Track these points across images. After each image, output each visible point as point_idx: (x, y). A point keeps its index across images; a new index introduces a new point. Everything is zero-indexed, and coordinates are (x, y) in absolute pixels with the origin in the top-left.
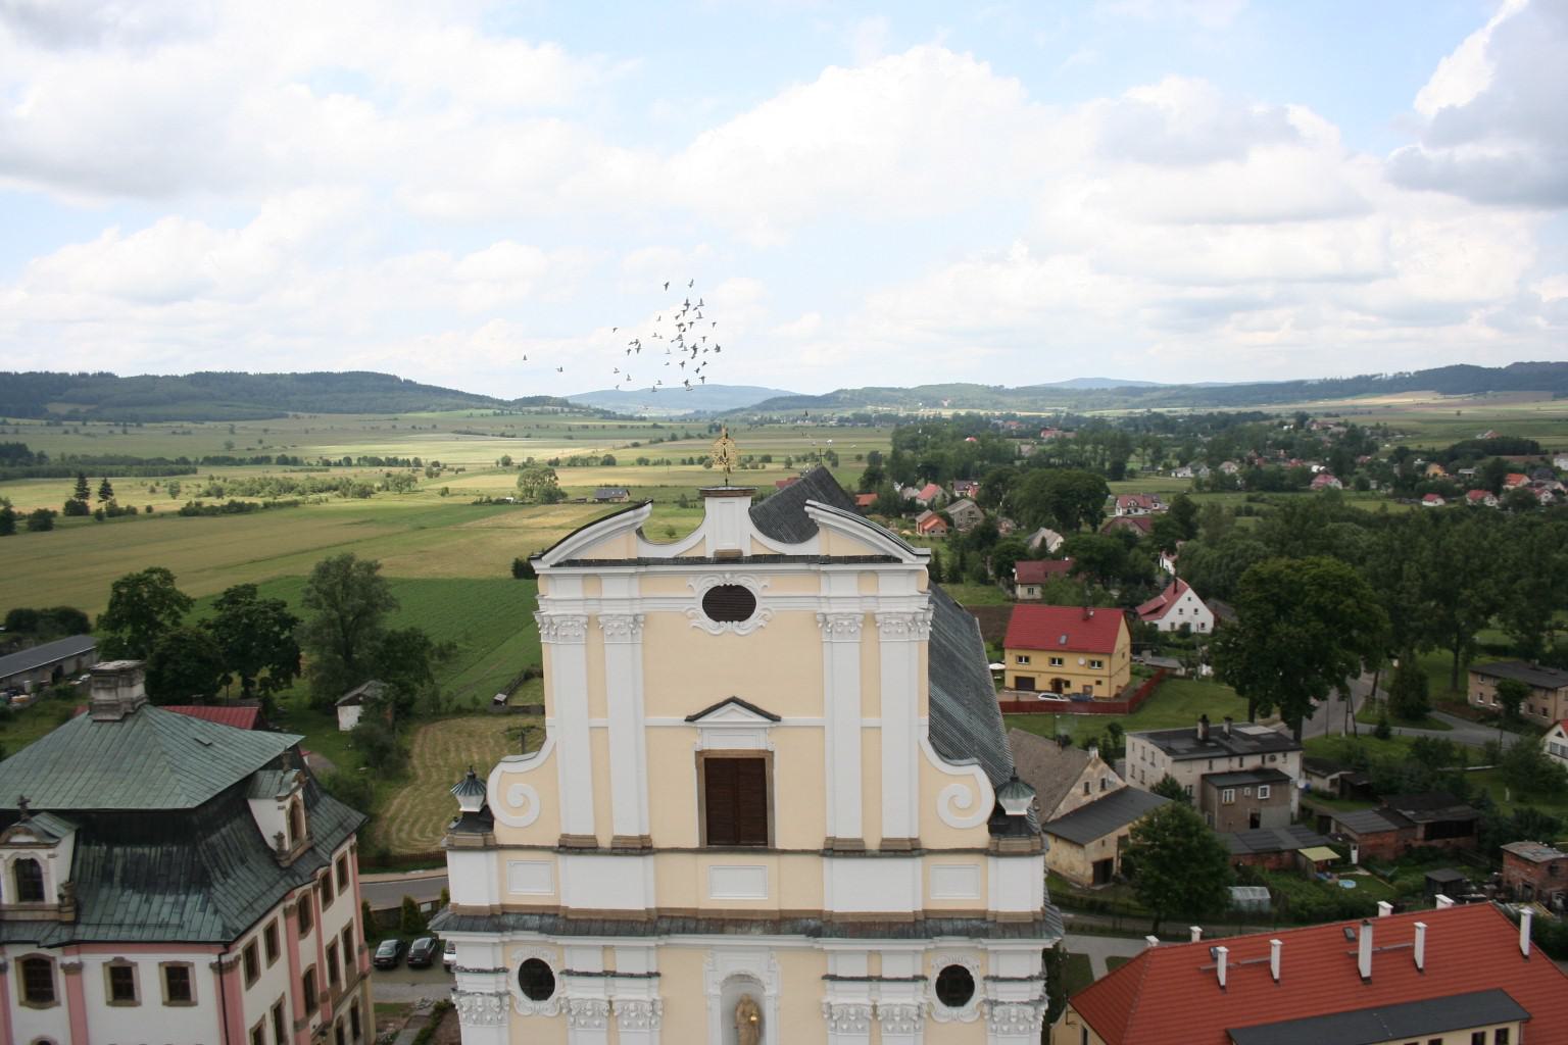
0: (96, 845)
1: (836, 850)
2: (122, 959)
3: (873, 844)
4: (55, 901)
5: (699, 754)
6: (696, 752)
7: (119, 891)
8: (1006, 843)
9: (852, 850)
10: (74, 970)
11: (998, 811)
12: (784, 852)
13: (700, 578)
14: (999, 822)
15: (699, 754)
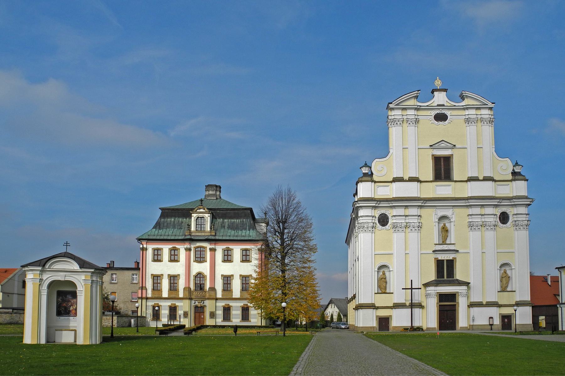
0: (219, 219)
1: (471, 179)
2: (229, 248)
3: (481, 178)
4: (209, 229)
5: (433, 155)
6: (432, 155)
7: (227, 230)
8: (517, 177)
9: (476, 179)
10: (213, 250)
11: (513, 170)
12: (456, 181)
13: (433, 111)
14: (514, 173)
15: (433, 155)
